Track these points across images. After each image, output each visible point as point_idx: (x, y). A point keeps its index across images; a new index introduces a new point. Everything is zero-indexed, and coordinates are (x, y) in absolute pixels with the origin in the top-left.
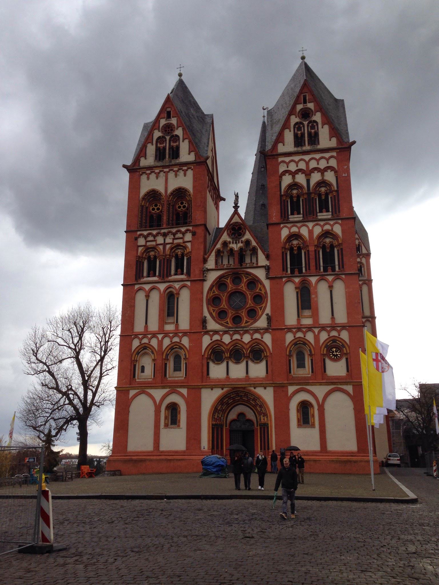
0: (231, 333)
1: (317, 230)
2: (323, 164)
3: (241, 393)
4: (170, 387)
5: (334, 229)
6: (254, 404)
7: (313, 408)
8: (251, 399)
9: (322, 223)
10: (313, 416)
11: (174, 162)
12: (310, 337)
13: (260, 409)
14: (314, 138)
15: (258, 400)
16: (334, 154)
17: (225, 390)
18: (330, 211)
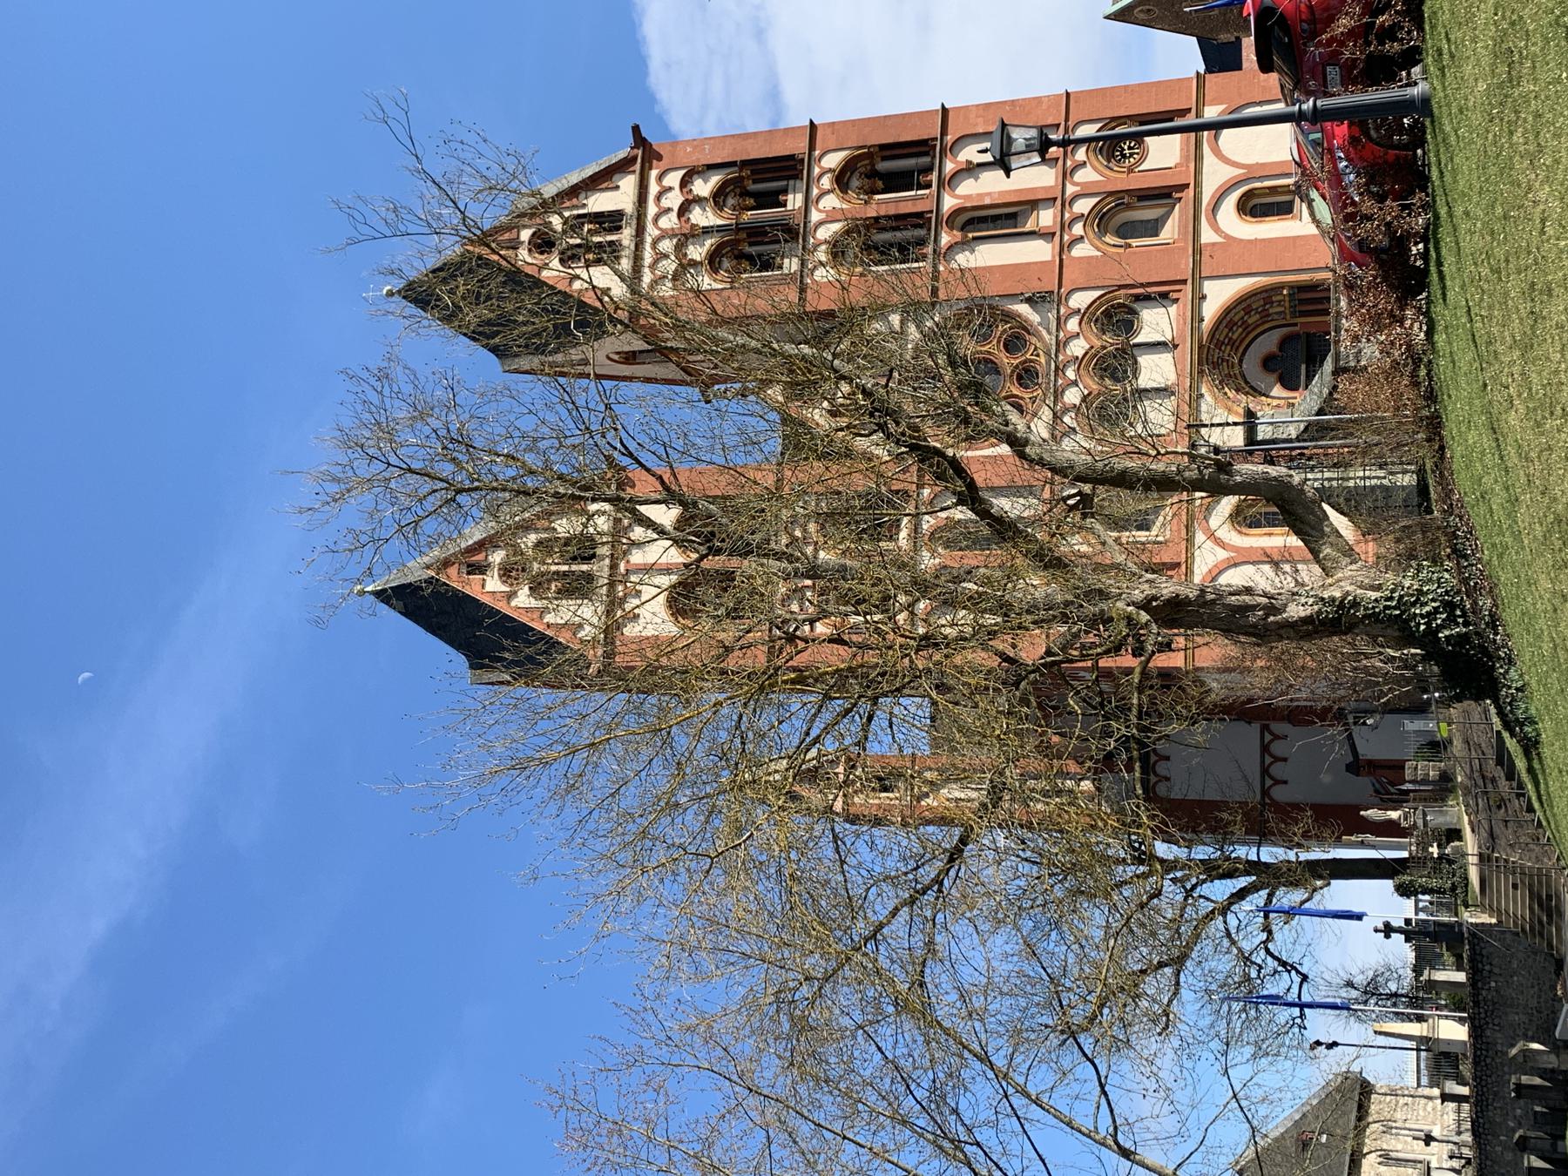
0: (1060, 382)
1: (831, 202)
2: (674, 200)
3: (1213, 356)
4: (1188, 527)
5: (833, 166)
6: (1240, 330)
7: (1256, 189)
8: (1227, 335)
9: (815, 192)
10: (1273, 190)
11: (604, 551)
12: (1084, 206)
13: (1253, 313)
14: (612, 220)
15: (1232, 314)
16: (654, 173)
17: (1204, 390)
18: (785, 183)
